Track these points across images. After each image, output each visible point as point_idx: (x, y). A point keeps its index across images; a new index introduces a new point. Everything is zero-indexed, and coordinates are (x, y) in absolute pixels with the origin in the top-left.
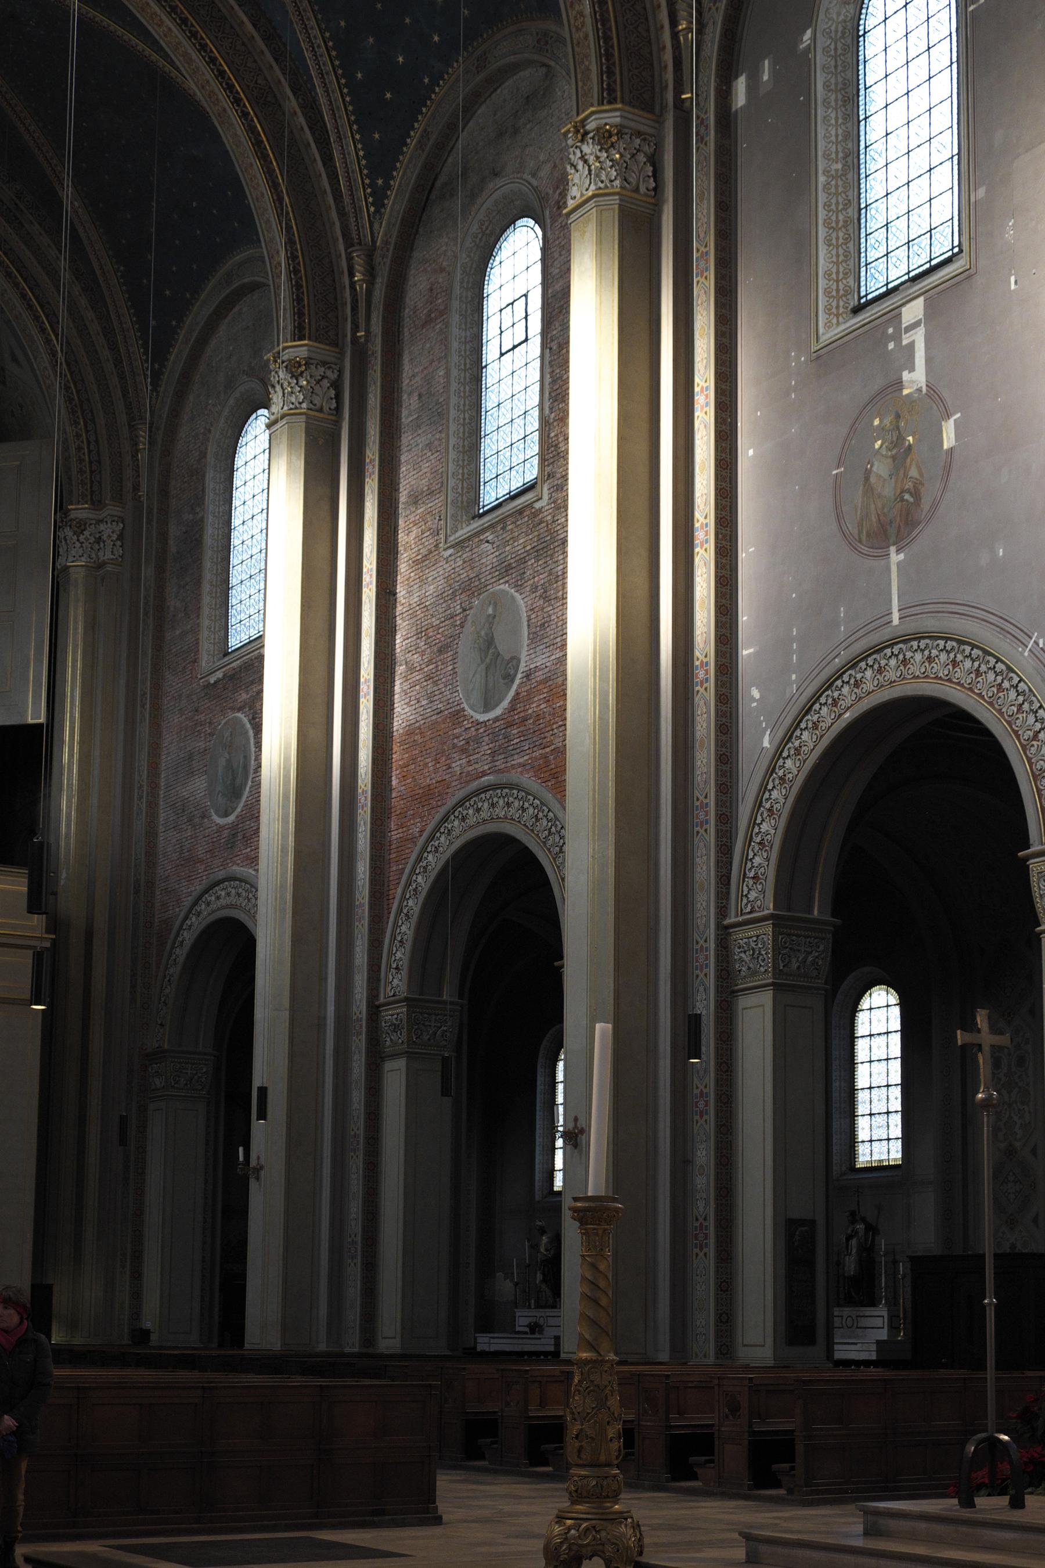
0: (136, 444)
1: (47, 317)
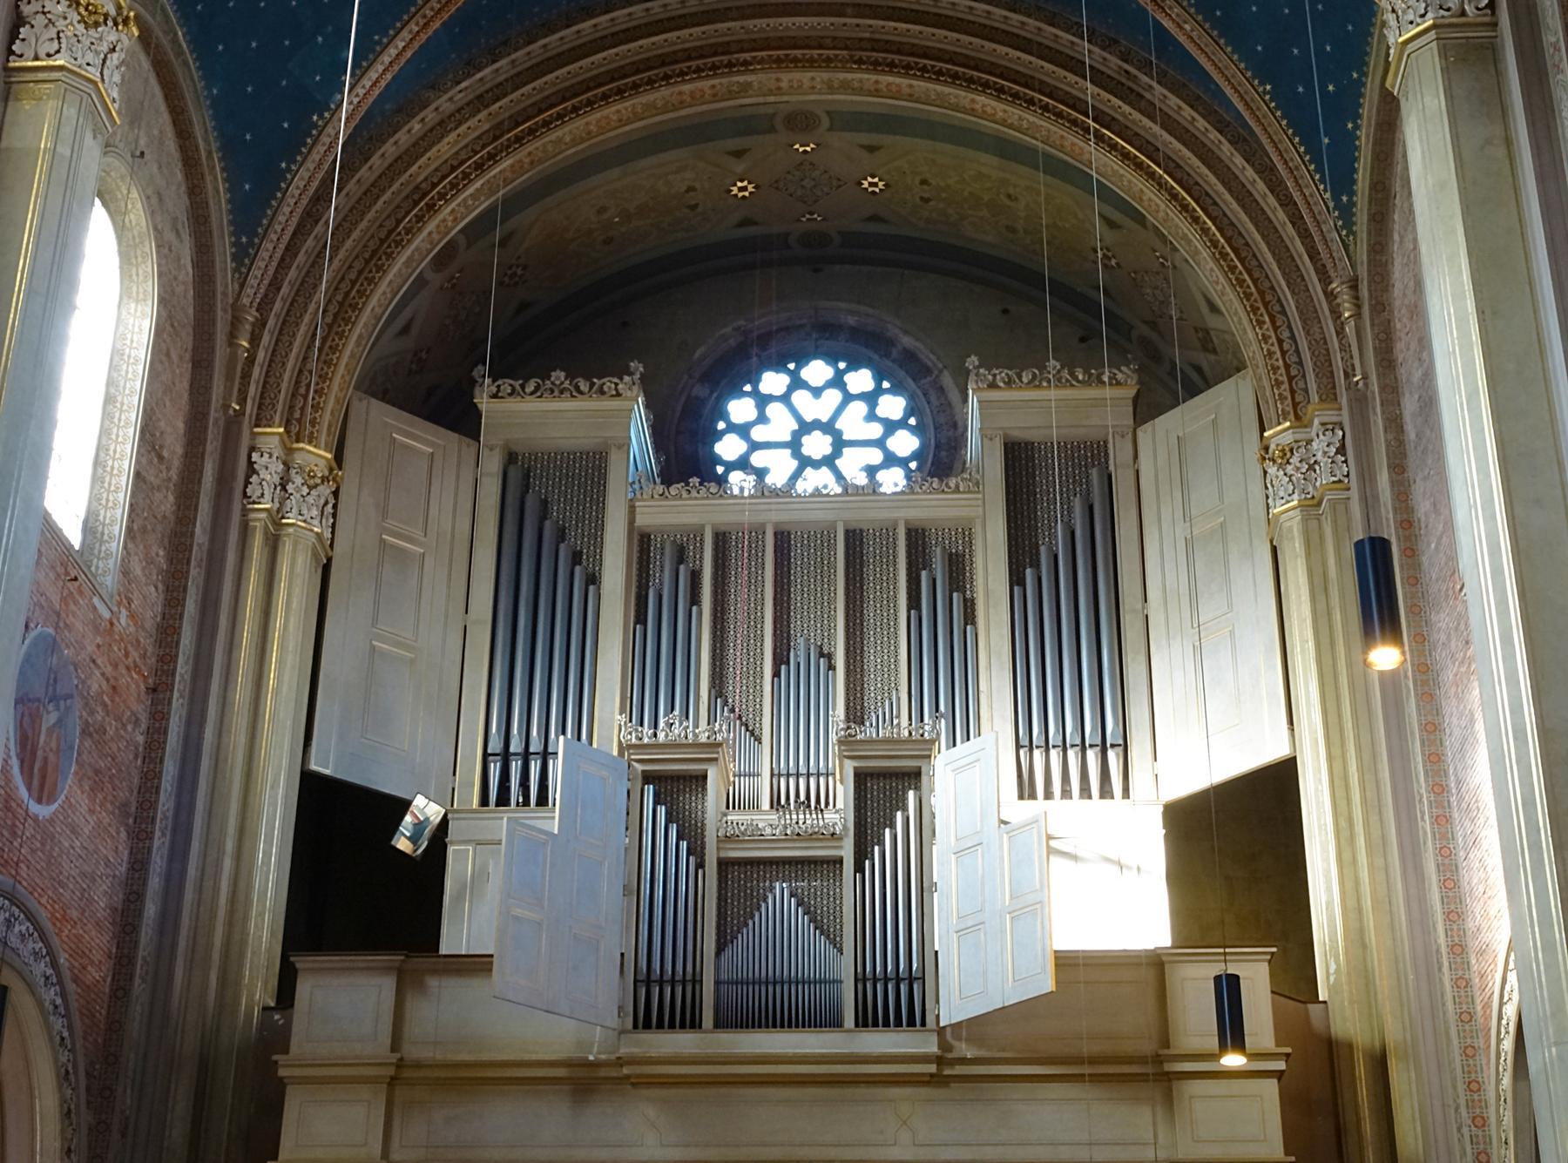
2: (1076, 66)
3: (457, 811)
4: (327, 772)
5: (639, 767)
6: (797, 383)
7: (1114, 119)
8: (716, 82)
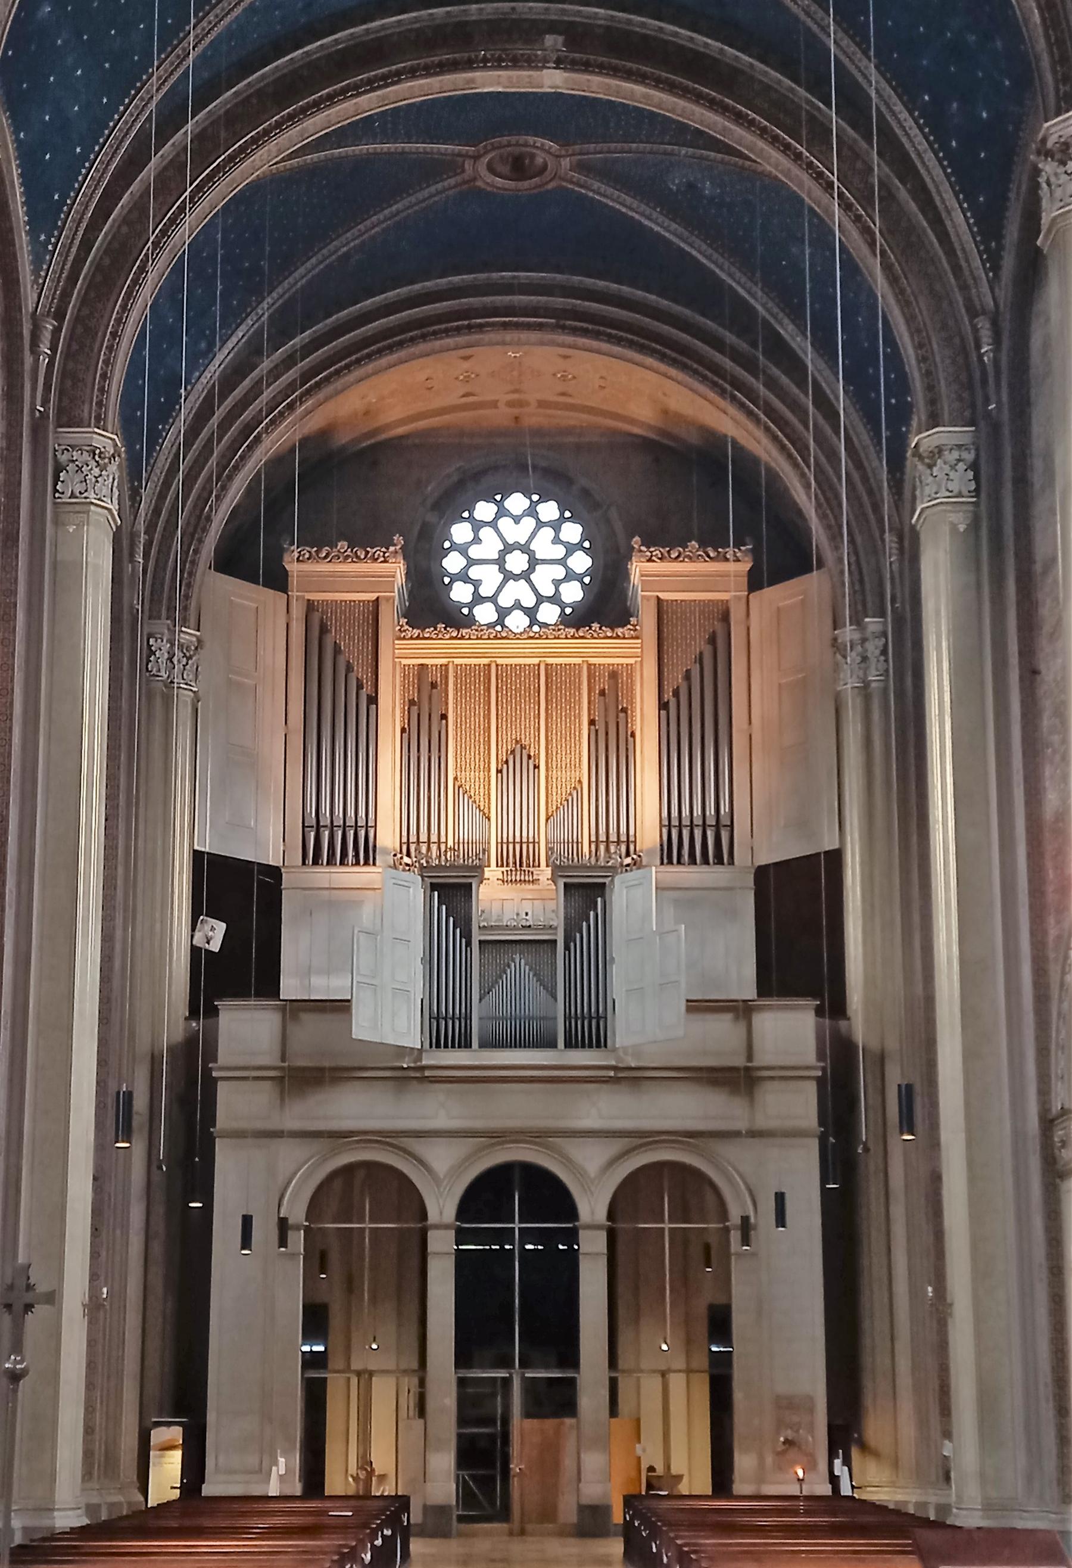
2: (718, 344)
5: (428, 881)
6: (502, 512)
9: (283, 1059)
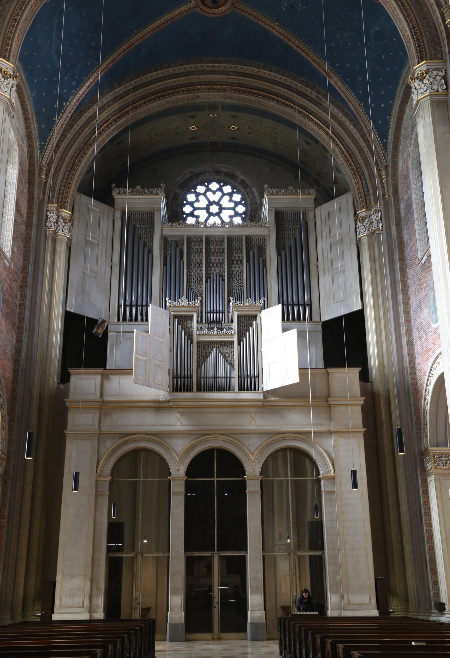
0: (382, 177)
1: (338, 139)
3: (111, 322)
4: (72, 311)
5: (173, 313)
6: (208, 189)
7: (313, 112)
8: (189, 95)
9: (101, 396)
